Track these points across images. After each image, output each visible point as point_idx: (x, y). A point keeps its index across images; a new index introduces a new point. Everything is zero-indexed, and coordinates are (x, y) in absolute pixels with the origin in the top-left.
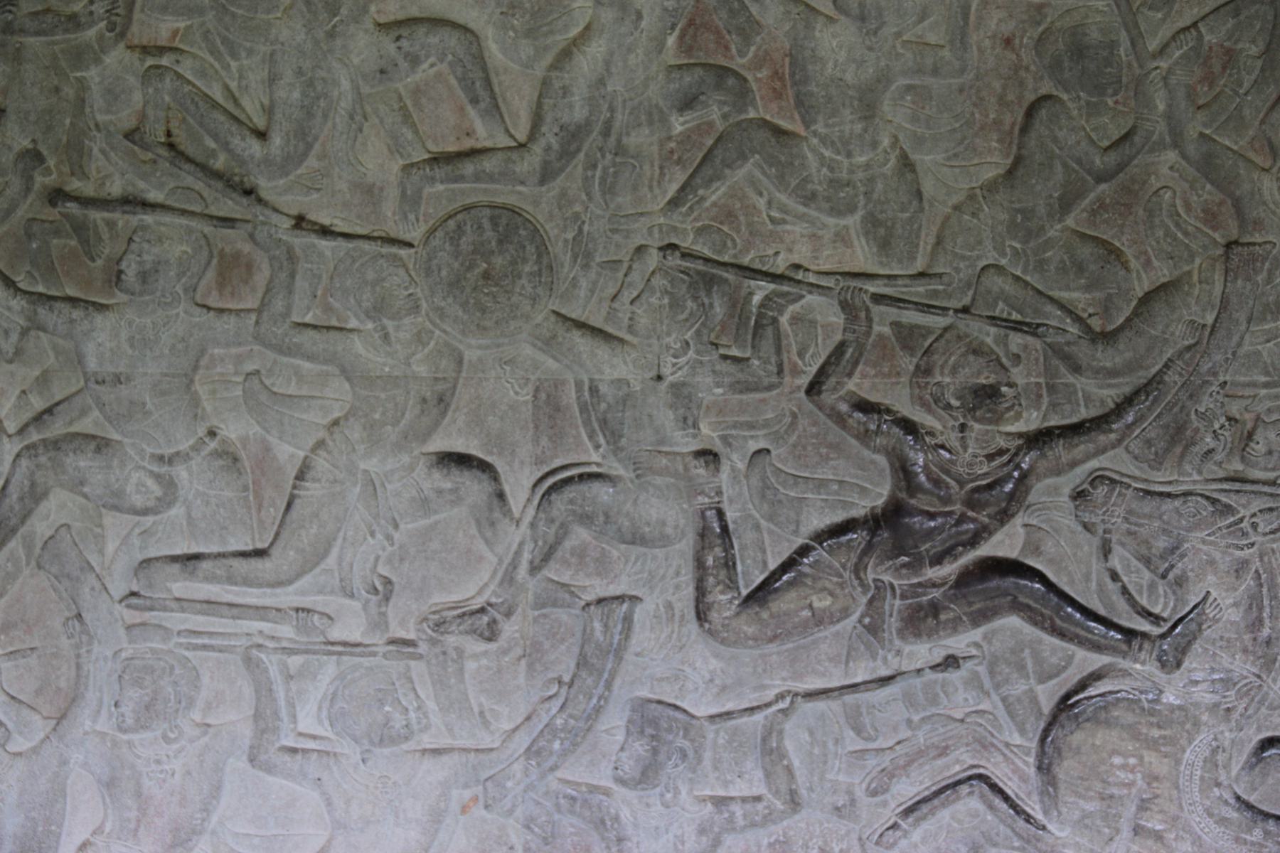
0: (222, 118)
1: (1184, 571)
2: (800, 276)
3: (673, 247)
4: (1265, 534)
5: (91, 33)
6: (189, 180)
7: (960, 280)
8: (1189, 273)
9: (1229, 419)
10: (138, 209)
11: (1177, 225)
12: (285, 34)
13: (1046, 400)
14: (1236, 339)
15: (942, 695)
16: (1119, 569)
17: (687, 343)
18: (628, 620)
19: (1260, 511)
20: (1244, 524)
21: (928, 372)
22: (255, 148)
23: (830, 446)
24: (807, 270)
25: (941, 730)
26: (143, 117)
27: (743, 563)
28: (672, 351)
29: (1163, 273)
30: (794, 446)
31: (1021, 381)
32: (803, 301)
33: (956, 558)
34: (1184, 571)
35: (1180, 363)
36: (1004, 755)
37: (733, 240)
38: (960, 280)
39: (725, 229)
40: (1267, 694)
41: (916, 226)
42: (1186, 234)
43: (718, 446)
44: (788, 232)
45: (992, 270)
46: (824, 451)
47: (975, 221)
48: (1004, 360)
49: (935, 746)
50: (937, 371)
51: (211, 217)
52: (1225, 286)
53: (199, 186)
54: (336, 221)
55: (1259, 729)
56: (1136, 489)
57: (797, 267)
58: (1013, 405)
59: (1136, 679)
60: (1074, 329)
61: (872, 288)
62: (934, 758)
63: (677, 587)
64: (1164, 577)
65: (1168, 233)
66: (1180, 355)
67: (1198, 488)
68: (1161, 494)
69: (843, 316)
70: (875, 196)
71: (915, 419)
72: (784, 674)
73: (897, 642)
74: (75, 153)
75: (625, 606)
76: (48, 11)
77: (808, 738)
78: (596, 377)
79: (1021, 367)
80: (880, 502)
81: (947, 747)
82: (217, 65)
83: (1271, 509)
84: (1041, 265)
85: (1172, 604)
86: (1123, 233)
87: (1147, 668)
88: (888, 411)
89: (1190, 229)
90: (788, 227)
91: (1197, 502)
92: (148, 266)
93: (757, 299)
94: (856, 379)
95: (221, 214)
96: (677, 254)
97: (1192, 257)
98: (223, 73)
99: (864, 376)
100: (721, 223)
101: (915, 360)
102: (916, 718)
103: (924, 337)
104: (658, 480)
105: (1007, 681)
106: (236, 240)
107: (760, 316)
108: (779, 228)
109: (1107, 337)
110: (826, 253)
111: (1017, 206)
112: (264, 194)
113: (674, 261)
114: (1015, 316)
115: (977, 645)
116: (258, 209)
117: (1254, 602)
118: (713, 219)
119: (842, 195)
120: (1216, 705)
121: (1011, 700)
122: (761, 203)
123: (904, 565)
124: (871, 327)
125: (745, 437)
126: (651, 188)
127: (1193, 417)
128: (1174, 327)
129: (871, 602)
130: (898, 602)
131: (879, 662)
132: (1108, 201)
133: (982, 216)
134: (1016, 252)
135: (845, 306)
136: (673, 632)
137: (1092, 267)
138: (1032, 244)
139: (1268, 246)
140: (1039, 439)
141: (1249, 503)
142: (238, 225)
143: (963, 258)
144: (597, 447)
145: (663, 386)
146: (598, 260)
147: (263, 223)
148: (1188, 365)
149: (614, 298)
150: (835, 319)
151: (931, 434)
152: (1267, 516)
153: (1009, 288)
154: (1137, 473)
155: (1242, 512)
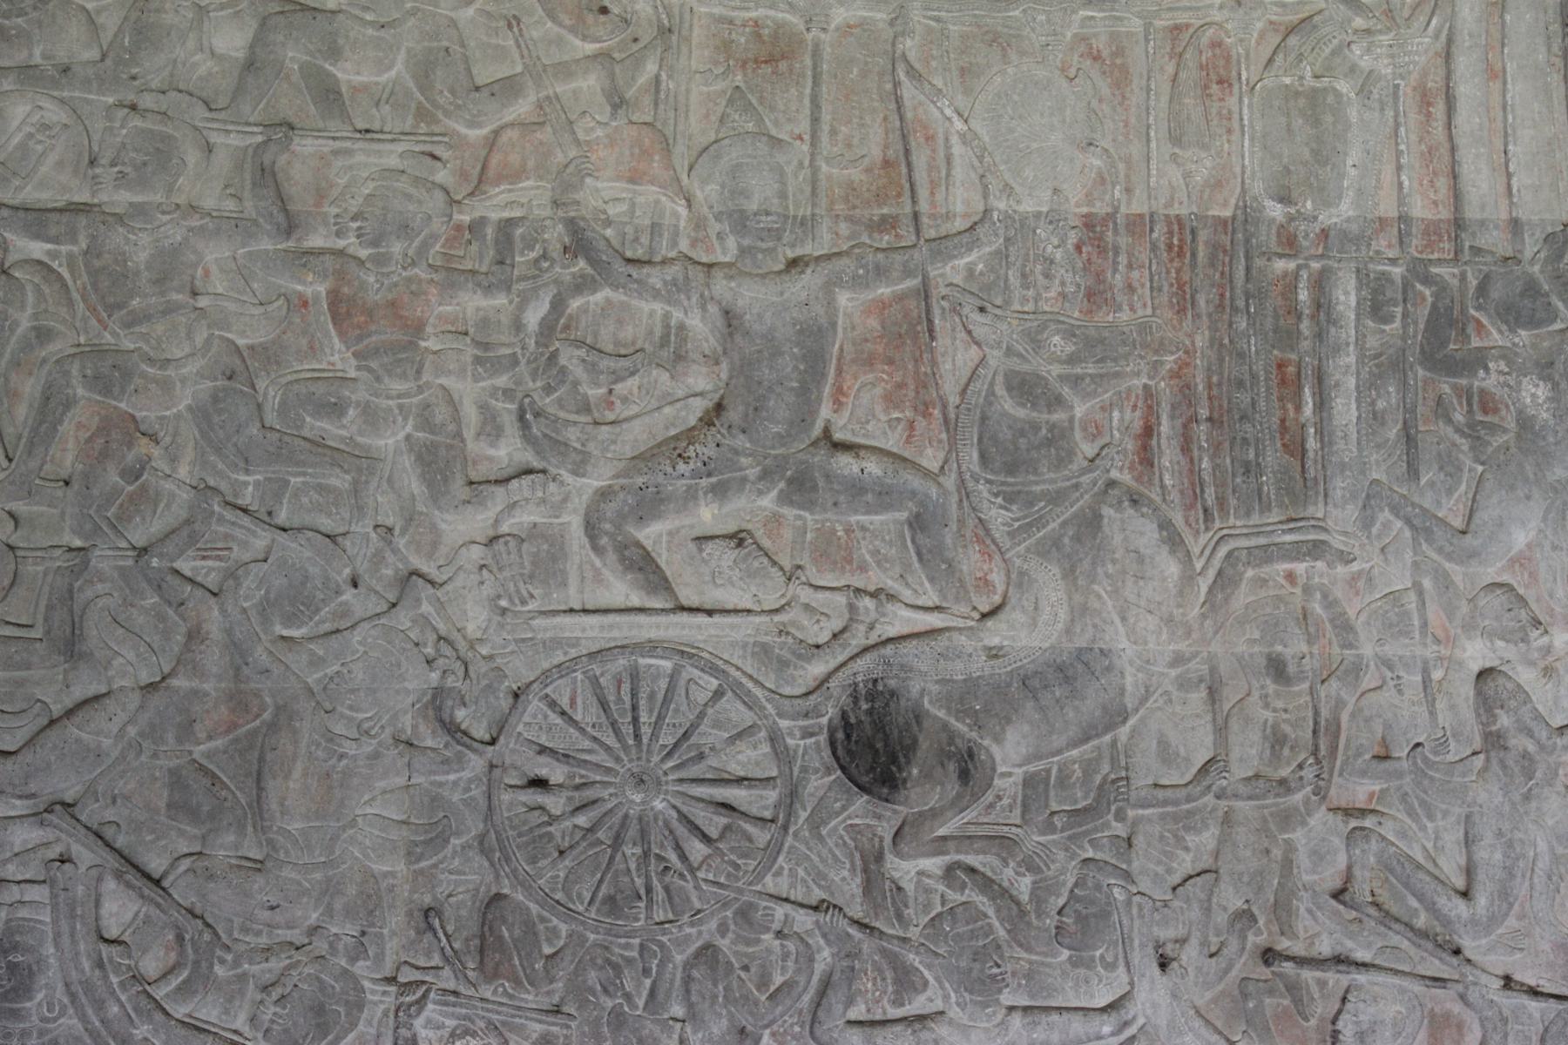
0: (1428, 879)
5: (1298, 797)
6: (1395, 940)
10: (1352, 968)
12: (1483, 797)
22: (1460, 908)
26: (1349, 877)
51: (1423, 977)
53: (1405, 944)
54: (1541, 982)
74: (1282, 911)
76: (1257, 776)
82: (1414, 826)
92: (1365, 1027)
95: (1429, 973)
98: (1420, 834)
106: (1446, 1000)
112: (1468, 953)
116: (1467, 969)
142: (1449, 985)
147: (1475, 984)
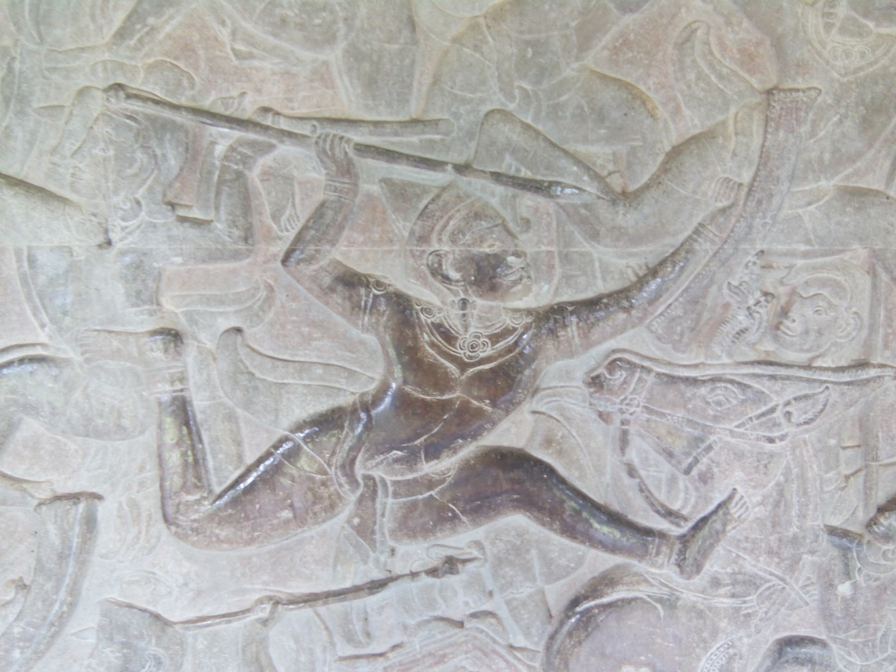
1: (709, 469)
2: (268, 121)
3: (119, 87)
4: (799, 425)
7: (460, 129)
8: (724, 123)
9: (766, 294)
11: (711, 66)
13: (558, 271)
14: (776, 201)
15: (440, 600)
16: (636, 462)
17: (138, 203)
18: (90, 522)
19: (795, 399)
20: (778, 415)
21: (423, 239)
23: (313, 324)
24: (278, 114)
25: (439, 637)
27: (214, 457)
28: (121, 213)
29: (693, 122)
30: (272, 324)
31: (530, 250)
32: (275, 153)
33: (455, 452)
34: (709, 469)
35: (712, 228)
36: (507, 662)
37: (191, 78)
38: (460, 129)
39: (181, 65)
40: (789, 595)
41: (407, 61)
42: (721, 77)
43: (182, 324)
44: (257, 69)
45: (498, 116)
46: (306, 330)
47: (478, 55)
48: (511, 225)
49: (431, 654)
50: (434, 237)
52: (765, 138)
55: (776, 630)
56: (659, 375)
57: (266, 110)
58: (521, 279)
59: (652, 585)
60: (592, 188)
61: (358, 137)
62: (431, 666)
63: (142, 484)
64: (687, 472)
65: (700, 77)
66: (713, 218)
67: (728, 372)
68: (686, 380)
69: (324, 172)
70: (358, 23)
71: (410, 293)
72: (265, 578)
73: (391, 543)
75: (82, 507)
77: (293, 645)
78: (34, 244)
79: (530, 234)
80: (372, 387)
81: (444, 656)
83: (806, 397)
84: (555, 111)
85: (693, 501)
86: (649, 75)
87: (664, 571)
88: (378, 284)
89: (725, 70)
90: (256, 63)
91: (726, 388)
93: (220, 149)
94: (342, 246)
96: (122, 94)
97: (727, 104)
99: (351, 243)
100: (176, 58)
101: (409, 225)
102: (412, 622)
103: (419, 197)
104: (112, 364)
105: (511, 584)
107: (224, 169)
108: (246, 64)
109: (626, 198)
110: (302, 94)
111: (528, 37)
113: (120, 104)
114: (525, 173)
115: (478, 544)
117: (780, 499)
118: (166, 54)
119: (317, 21)
120: (737, 610)
121: (515, 603)
122: (224, 34)
123: (397, 460)
124: (356, 185)
125: (212, 313)
126: (93, 17)
127: (725, 291)
128: (704, 190)
129: (360, 501)
130: (390, 500)
131: (371, 565)
132: (632, 37)
133: (485, 49)
134: (526, 94)
135: (325, 155)
136: (140, 532)
137: (615, 114)
138: (545, 85)
139: (813, 93)
140: (551, 318)
141: (783, 389)
143: (464, 101)
144: (43, 326)
145: (112, 253)
146: (35, 105)
148: (721, 231)
149: (54, 151)
150: (314, 175)
151: (428, 311)
152: (802, 404)
153: (517, 137)
154: (658, 354)
155: (776, 400)
